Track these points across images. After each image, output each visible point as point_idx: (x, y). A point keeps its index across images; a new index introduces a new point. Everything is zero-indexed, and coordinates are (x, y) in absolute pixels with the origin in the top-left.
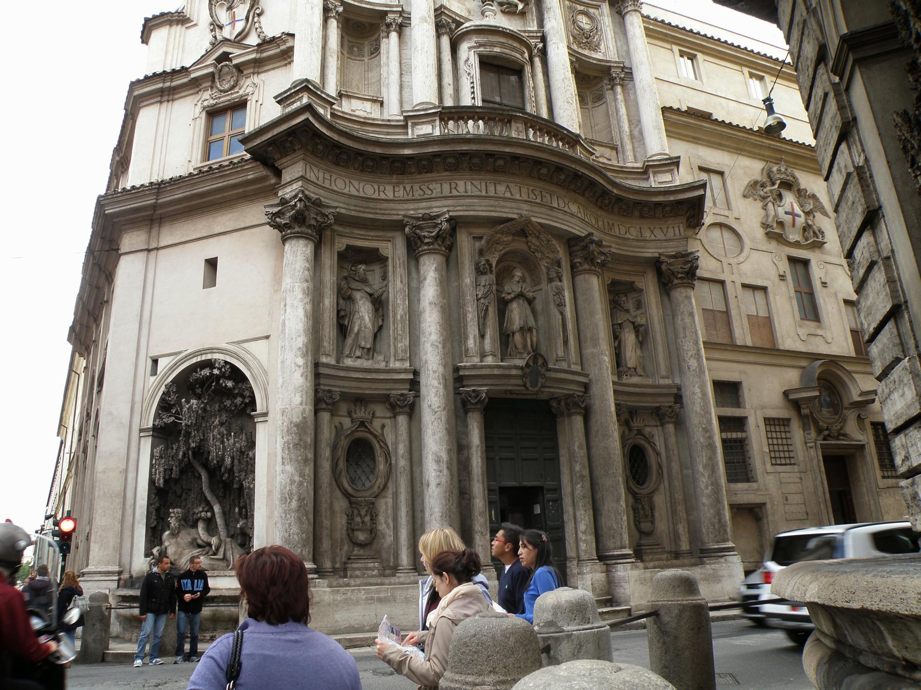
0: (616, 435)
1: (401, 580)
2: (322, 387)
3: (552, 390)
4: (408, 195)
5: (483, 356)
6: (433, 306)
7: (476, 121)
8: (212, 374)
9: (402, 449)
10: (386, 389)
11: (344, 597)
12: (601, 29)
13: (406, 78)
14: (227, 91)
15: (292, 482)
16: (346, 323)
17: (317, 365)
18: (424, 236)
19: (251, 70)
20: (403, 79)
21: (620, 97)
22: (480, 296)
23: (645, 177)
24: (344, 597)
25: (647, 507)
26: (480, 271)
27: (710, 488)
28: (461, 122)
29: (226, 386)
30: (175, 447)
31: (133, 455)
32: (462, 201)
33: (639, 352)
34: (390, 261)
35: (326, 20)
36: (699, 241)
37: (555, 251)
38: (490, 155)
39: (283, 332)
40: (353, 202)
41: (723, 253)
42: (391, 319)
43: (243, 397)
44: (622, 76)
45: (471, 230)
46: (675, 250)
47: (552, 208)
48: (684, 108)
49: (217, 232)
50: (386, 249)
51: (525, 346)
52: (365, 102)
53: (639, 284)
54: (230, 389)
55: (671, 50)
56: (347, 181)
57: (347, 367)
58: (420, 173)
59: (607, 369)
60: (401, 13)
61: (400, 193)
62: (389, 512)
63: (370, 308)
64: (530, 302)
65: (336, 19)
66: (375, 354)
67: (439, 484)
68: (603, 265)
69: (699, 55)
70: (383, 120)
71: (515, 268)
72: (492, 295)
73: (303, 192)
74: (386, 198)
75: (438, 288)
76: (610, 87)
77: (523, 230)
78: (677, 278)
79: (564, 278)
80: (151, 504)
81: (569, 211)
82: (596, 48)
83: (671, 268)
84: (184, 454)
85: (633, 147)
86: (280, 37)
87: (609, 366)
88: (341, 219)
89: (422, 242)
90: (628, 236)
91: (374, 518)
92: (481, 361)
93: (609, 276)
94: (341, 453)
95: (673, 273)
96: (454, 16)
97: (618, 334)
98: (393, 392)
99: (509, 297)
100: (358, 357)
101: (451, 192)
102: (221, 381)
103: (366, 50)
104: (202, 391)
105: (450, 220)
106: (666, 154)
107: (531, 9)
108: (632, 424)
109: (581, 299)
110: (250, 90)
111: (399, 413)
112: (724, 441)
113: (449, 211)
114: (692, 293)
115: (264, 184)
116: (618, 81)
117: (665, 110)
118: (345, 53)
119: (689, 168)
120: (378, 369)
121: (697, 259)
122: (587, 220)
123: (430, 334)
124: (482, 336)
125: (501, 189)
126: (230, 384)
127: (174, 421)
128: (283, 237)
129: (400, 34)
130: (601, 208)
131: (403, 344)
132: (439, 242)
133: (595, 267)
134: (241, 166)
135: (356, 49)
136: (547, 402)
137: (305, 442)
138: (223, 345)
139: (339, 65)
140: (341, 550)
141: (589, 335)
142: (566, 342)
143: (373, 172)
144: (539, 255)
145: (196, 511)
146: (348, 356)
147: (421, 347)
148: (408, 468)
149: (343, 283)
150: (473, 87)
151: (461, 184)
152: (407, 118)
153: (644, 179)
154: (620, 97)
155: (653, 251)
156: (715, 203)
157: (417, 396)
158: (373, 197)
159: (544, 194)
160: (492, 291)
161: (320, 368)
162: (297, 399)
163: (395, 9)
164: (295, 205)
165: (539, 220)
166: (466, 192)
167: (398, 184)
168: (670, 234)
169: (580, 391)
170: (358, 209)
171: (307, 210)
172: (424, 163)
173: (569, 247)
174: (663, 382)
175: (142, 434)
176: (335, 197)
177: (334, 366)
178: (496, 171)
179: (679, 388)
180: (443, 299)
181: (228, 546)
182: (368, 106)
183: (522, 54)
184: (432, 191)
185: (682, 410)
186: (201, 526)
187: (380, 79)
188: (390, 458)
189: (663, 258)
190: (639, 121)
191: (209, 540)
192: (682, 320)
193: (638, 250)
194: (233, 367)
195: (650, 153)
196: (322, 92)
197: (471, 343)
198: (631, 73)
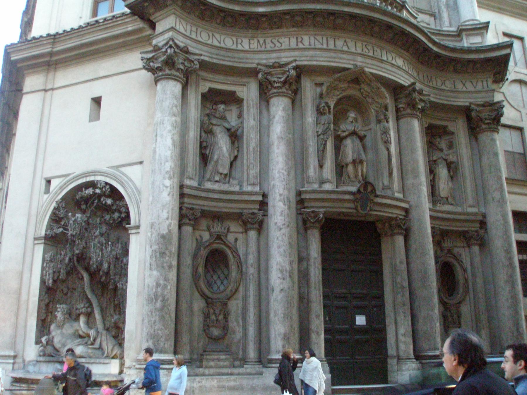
0: (432, 253)
1: (248, 370)
2: (186, 205)
4: (261, 47)
6: (281, 140)
8: (95, 194)
9: (251, 259)
10: (240, 209)
11: (199, 384)
15: (158, 285)
16: (207, 152)
17: (182, 187)
18: (274, 81)
22: (320, 133)
23: (459, 39)
24: (199, 384)
25: (455, 316)
27: (510, 301)
29: (106, 203)
30: (63, 253)
31: (28, 259)
32: (306, 53)
33: (450, 184)
34: (245, 102)
36: (502, 94)
37: (383, 97)
39: (154, 158)
40: (215, 51)
41: (522, 105)
42: (245, 151)
43: (120, 212)
45: (313, 78)
47: (382, 61)
49: (101, 75)
50: (241, 92)
51: (356, 176)
53: (451, 127)
54: (109, 206)
56: (211, 35)
58: (272, 28)
59: (425, 198)
61: (255, 45)
62: (239, 312)
63: (228, 141)
64: (362, 139)
66: (231, 180)
67: (282, 290)
68: (422, 110)
72: (330, 132)
73: (173, 41)
75: (285, 125)
77: (357, 78)
78: (484, 124)
79: (390, 120)
80: (42, 300)
81: (396, 64)
83: (480, 115)
84: (70, 260)
85: (449, 15)
87: (426, 194)
88: (204, 65)
89: (272, 86)
90: (443, 87)
91: (226, 317)
92: (320, 187)
93: (427, 122)
94: (201, 261)
95: (481, 119)
97: (433, 169)
98: (245, 211)
99: (344, 134)
100: (217, 181)
101: (297, 45)
102: (102, 199)
104: (87, 207)
105: (296, 68)
106: (477, 20)
109: (403, 137)
111: (250, 229)
112: (521, 262)
113: (295, 61)
114: (496, 136)
115: (140, 35)
119: (495, 34)
120: (233, 192)
121: (502, 108)
122: (410, 72)
123: (278, 163)
124: (321, 166)
125: (340, 43)
126: (109, 201)
127: (62, 232)
128: (156, 78)
130: (422, 63)
131: (254, 171)
132: (287, 86)
133: (416, 112)
134: (122, 20)
136: (373, 223)
137: (170, 252)
138: (104, 169)
140: (198, 343)
141: (409, 168)
142: (391, 174)
144: (370, 100)
145: (79, 307)
146: (209, 180)
147: (270, 173)
148: (256, 276)
149: (206, 118)
151: (306, 38)
155: (465, 100)
156: (516, 64)
157: (265, 215)
158: (232, 48)
159: (375, 49)
160: (330, 129)
161: (185, 189)
162: (165, 215)
164: (166, 51)
165: (371, 71)
167: (253, 37)
168: (479, 87)
171: (176, 56)
172: (275, 20)
174: (470, 210)
175: (36, 242)
176: (200, 46)
177: (196, 187)
178: (335, 28)
179: (484, 216)
180: (289, 134)
181: (104, 338)
186: (82, 319)
188: (242, 266)
189: (472, 106)
191: (88, 332)
192: (488, 158)
194: (112, 187)
195: (463, 20)
197: (311, 172)
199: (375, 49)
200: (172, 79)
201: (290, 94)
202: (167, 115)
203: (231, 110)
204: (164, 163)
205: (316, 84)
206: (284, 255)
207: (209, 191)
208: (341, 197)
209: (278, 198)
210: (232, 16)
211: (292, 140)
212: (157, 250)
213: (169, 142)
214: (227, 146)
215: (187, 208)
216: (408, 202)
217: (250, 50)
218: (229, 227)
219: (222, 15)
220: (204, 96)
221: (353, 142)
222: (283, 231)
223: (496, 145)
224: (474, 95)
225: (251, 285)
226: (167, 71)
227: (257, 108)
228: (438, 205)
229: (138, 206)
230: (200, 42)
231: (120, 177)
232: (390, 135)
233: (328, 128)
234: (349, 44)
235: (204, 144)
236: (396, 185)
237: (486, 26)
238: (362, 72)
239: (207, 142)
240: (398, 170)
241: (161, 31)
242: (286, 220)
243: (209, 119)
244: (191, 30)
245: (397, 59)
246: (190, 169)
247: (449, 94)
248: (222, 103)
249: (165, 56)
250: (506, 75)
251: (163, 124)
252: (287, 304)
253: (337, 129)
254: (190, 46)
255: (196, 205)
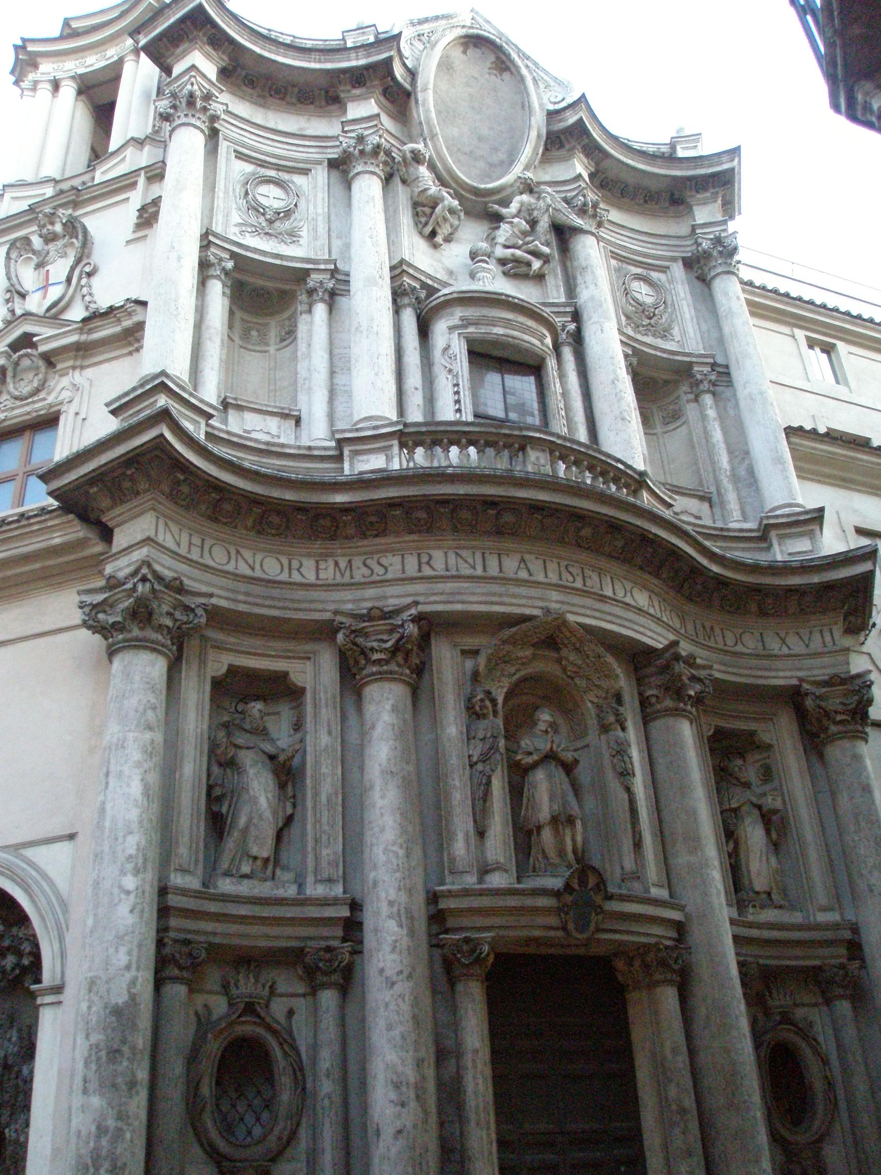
0: (744, 1024)
2: (172, 934)
3: (617, 937)
4: (342, 575)
5: (485, 871)
7: (463, 447)
9: (327, 1059)
12: (673, 304)
13: (340, 380)
14: (26, 398)
15: (101, 1130)
16: (224, 810)
17: (163, 891)
18: (372, 649)
19: (71, 363)
20: (336, 381)
21: (711, 413)
22: (475, 759)
23: (764, 545)
26: (476, 713)
28: (438, 450)
32: (440, 586)
33: (773, 860)
34: (309, 695)
35: (202, 282)
36: (866, 657)
38: (491, 503)
39: (100, 826)
40: (243, 587)
42: (309, 804)
44: (713, 377)
46: (829, 671)
47: (603, 598)
48: (822, 430)
51: (562, 853)
52: (268, 418)
53: (765, 737)
55: (793, 337)
57: (223, 895)
58: (364, 536)
59: (718, 894)
60: (334, 272)
61: (328, 573)
63: (271, 782)
64: (569, 768)
65: (220, 279)
66: (278, 872)
67: (399, 1132)
68: (698, 701)
69: (841, 346)
70: (299, 447)
71: (537, 708)
72: (498, 756)
73: (149, 566)
74: (303, 581)
76: (692, 396)
78: (836, 723)
79: (630, 725)
81: (633, 603)
82: (665, 333)
83: (823, 704)
86: (122, 306)
87: (721, 887)
89: (368, 660)
90: (739, 648)
92: (481, 881)
93: (711, 724)
94: (207, 1068)
95: (827, 714)
96: (423, 278)
99: (530, 760)
101: (420, 571)
103: (273, 334)
105: (418, 619)
106: (798, 505)
107: (554, 270)
108: (770, 1002)
109: (661, 762)
110: (66, 395)
111: (324, 986)
113: (416, 603)
114: (863, 749)
116: (705, 386)
117: (790, 431)
118: (236, 338)
119: (839, 531)
121: (869, 686)
122: (665, 619)
123: (382, 830)
124: (481, 834)
125: (511, 564)
128: (109, 646)
129: (331, 308)
130: (690, 599)
131: (331, 851)
132: (400, 658)
133: (685, 704)
135: (254, 333)
137: (133, 1048)
139: (224, 357)
142: (638, 845)
143: (279, 535)
144: (581, 683)
146: (227, 874)
147: (366, 855)
148: (337, 1100)
149: (222, 734)
150: (457, 393)
151: (438, 557)
152: (341, 443)
153: (761, 550)
154: (711, 413)
155: (788, 674)
157: (357, 952)
158: (279, 578)
159: (588, 573)
160: (497, 750)
161: (170, 896)
162: (122, 958)
163: (322, 267)
164: (134, 589)
166: (447, 570)
167: (325, 556)
168: (816, 644)
169: (670, 938)
170: (251, 599)
171: (156, 598)
172: (373, 519)
173: (636, 669)
174: (822, 917)
176: (207, 577)
178: (499, 532)
179: (855, 929)
180: (407, 763)
182: (273, 424)
183: (541, 339)
184: (386, 569)
185: (863, 972)
187: (296, 381)
188: (303, 1075)
189: (806, 686)
190: (747, 453)
192: (852, 798)
193: (759, 673)
196: (191, 394)
197: (459, 847)
198: (728, 374)
199: (588, 573)
200: (146, 648)
201: (406, 675)
202: (133, 728)
203: (278, 713)
204: (124, 837)
205: (463, 652)
206: (402, 1047)
207: (224, 898)
208: (529, 902)
209: (385, 910)
210: (278, 513)
211: (413, 777)
212: (102, 1044)
213: (136, 789)
214: (270, 795)
215: (176, 941)
216: (681, 908)
217: (319, 582)
218: (274, 983)
219: (257, 510)
220: (218, 684)
221: (550, 777)
222: (398, 988)
223: (865, 768)
224: (808, 662)
225: (327, 1125)
226: (136, 632)
227: (335, 708)
228: (751, 910)
229: (61, 939)
230: (207, 566)
231: (23, 870)
232: (630, 758)
233: (493, 748)
234: (531, 566)
235: (217, 791)
236: (652, 870)
237: (817, 517)
238: (561, 623)
239: (222, 786)
240: (653, 834)
241: (125, 545)
242: (405, 961)
243: (229, 735)
244: (190, 544)
245: (636, 592)
246: (183, 851)
247: (754, 662)
248: (257, 698)
249: (131, 600)
250: (870, 616)
251: (123, 747)
252: (414, 1166)
253: (515, 747)
254: (189, 578)
255: (196, 932)
